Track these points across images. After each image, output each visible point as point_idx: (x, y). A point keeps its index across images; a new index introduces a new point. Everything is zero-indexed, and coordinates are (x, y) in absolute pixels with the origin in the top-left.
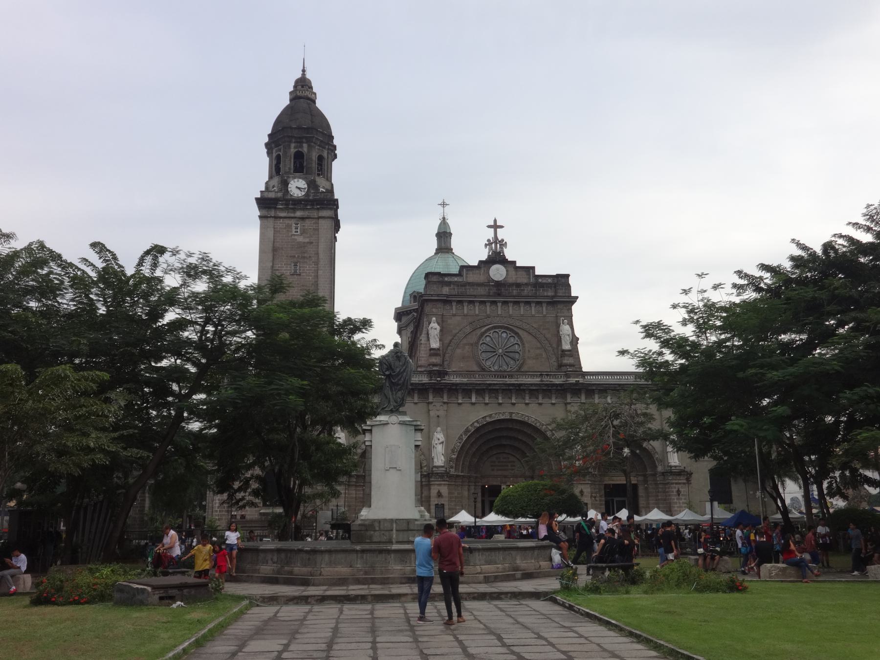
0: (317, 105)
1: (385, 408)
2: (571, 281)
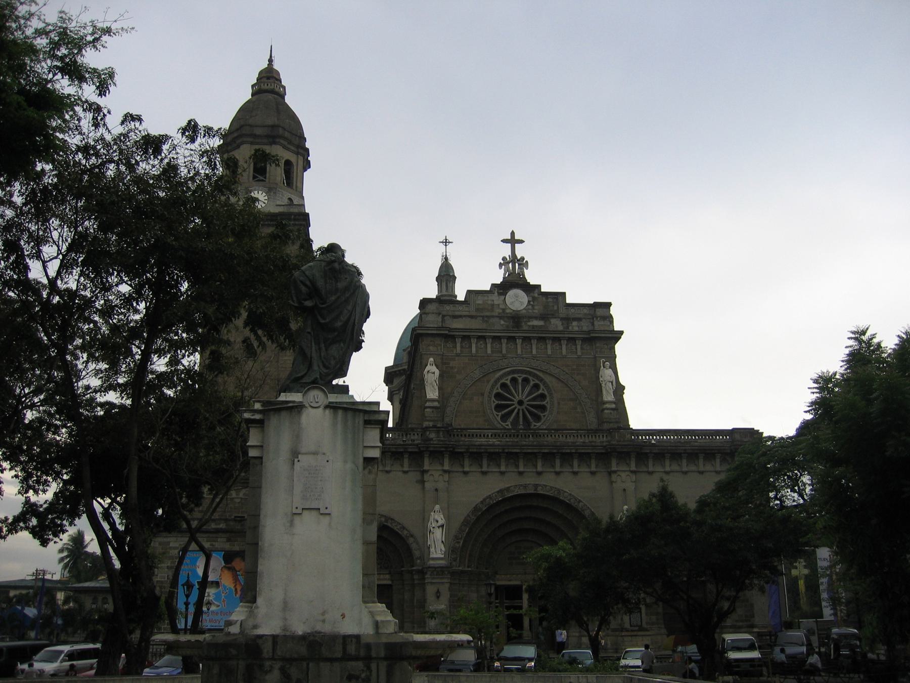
0: (286, 101)
1: (302, 377)
2: (613, 311)
